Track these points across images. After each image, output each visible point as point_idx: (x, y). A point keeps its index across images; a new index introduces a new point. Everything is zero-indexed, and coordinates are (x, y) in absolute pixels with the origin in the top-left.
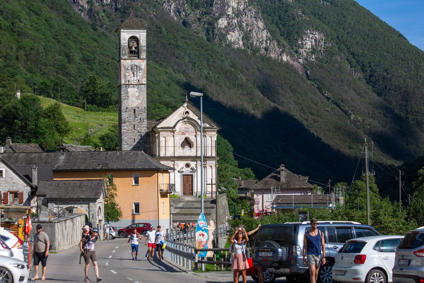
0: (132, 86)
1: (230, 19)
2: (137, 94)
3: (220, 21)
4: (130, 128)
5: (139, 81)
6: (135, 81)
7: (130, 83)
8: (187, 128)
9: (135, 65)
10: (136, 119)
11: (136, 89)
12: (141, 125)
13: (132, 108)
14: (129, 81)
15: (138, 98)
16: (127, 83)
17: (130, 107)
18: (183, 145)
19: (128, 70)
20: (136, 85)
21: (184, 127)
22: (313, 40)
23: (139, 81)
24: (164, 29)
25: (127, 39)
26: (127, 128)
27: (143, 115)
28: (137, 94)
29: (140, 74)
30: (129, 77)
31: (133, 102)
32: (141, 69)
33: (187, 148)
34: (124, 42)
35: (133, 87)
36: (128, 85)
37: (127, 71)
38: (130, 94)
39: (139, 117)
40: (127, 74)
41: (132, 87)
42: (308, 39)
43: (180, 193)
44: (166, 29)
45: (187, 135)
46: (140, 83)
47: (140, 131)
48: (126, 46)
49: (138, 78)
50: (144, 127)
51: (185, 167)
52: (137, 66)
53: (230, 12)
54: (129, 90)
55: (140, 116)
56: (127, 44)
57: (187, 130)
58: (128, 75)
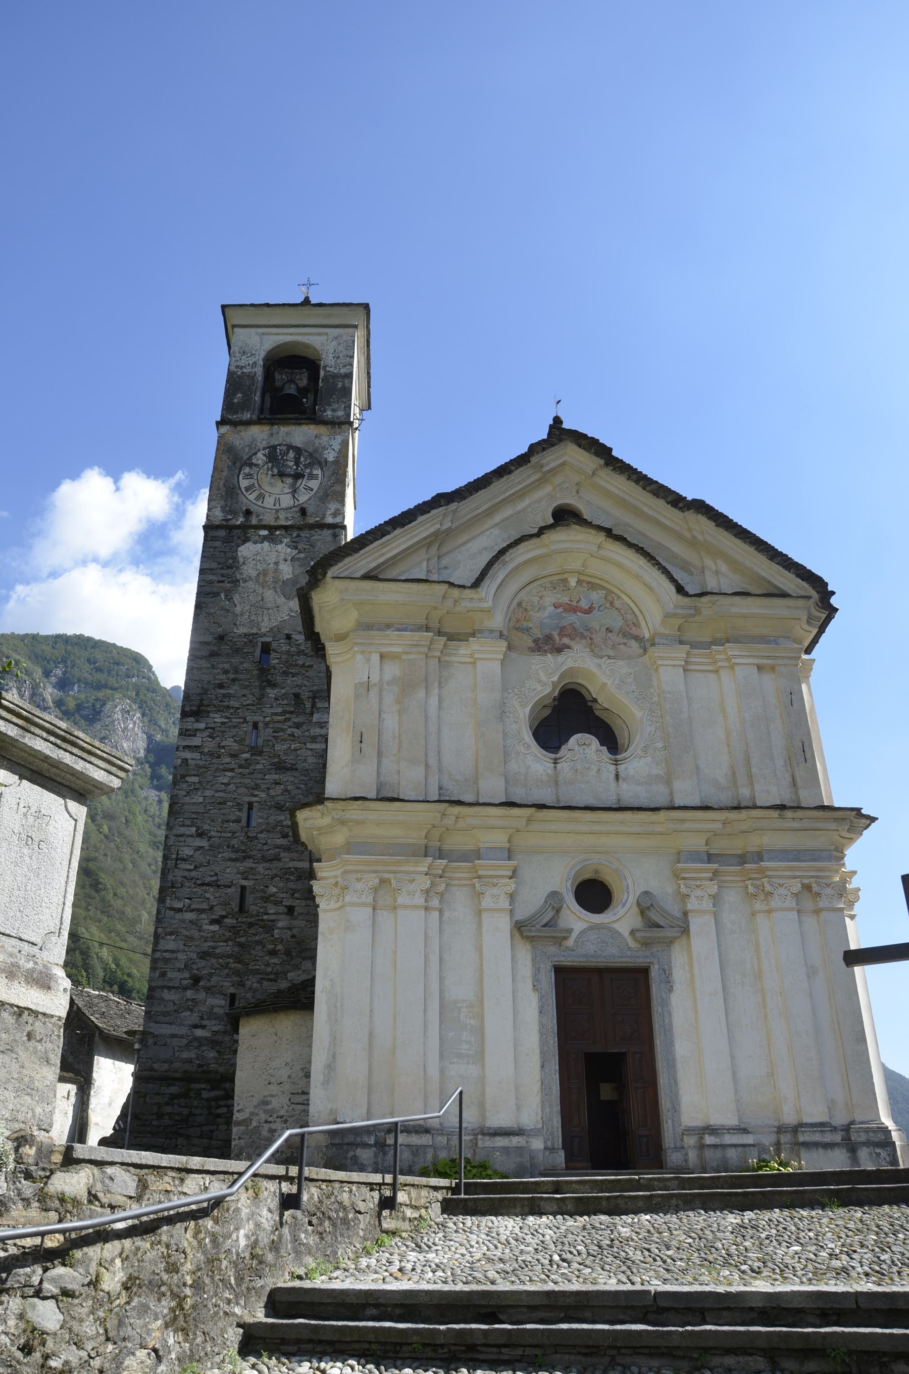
0: (265, 533)
4: (229, 742)
5: (303, 512)
6: (282, 515)
7: (254, 521)
8: (574, 610)
9: (290, 447)
10: (272, 693)
11: (283, 549)
12: (298, 726)
13: (251, 638)
14: (248, 513)
16: (240, 520)
17: (242, 630)
19: (251, 465)
20: (286, 528)
21: (550, 599)
23: (303, 512)
25: (263, 354)
26: (210, 745)
27: (310, 673)
29: (314, 484)
30: (252, 497)
31: (261, 606)
33: (583, 748)
34: (241, 364)
35: (271, 539)
36: (245, 527)
37: (247, 470)
38: (249, 570)
40: (244, 483)
41: (265, 538)
43: (537, 1144)
46: (311, 521)
47: (290, 759)
48: (252, 377)
49: (303, 498)
50: (314, 739)
51: (570, 900)
52: (298, 451)
54: (246, 550)
55: (298, 680)
56: (259, 371)
57: (572, 618)
58: (248, 489)
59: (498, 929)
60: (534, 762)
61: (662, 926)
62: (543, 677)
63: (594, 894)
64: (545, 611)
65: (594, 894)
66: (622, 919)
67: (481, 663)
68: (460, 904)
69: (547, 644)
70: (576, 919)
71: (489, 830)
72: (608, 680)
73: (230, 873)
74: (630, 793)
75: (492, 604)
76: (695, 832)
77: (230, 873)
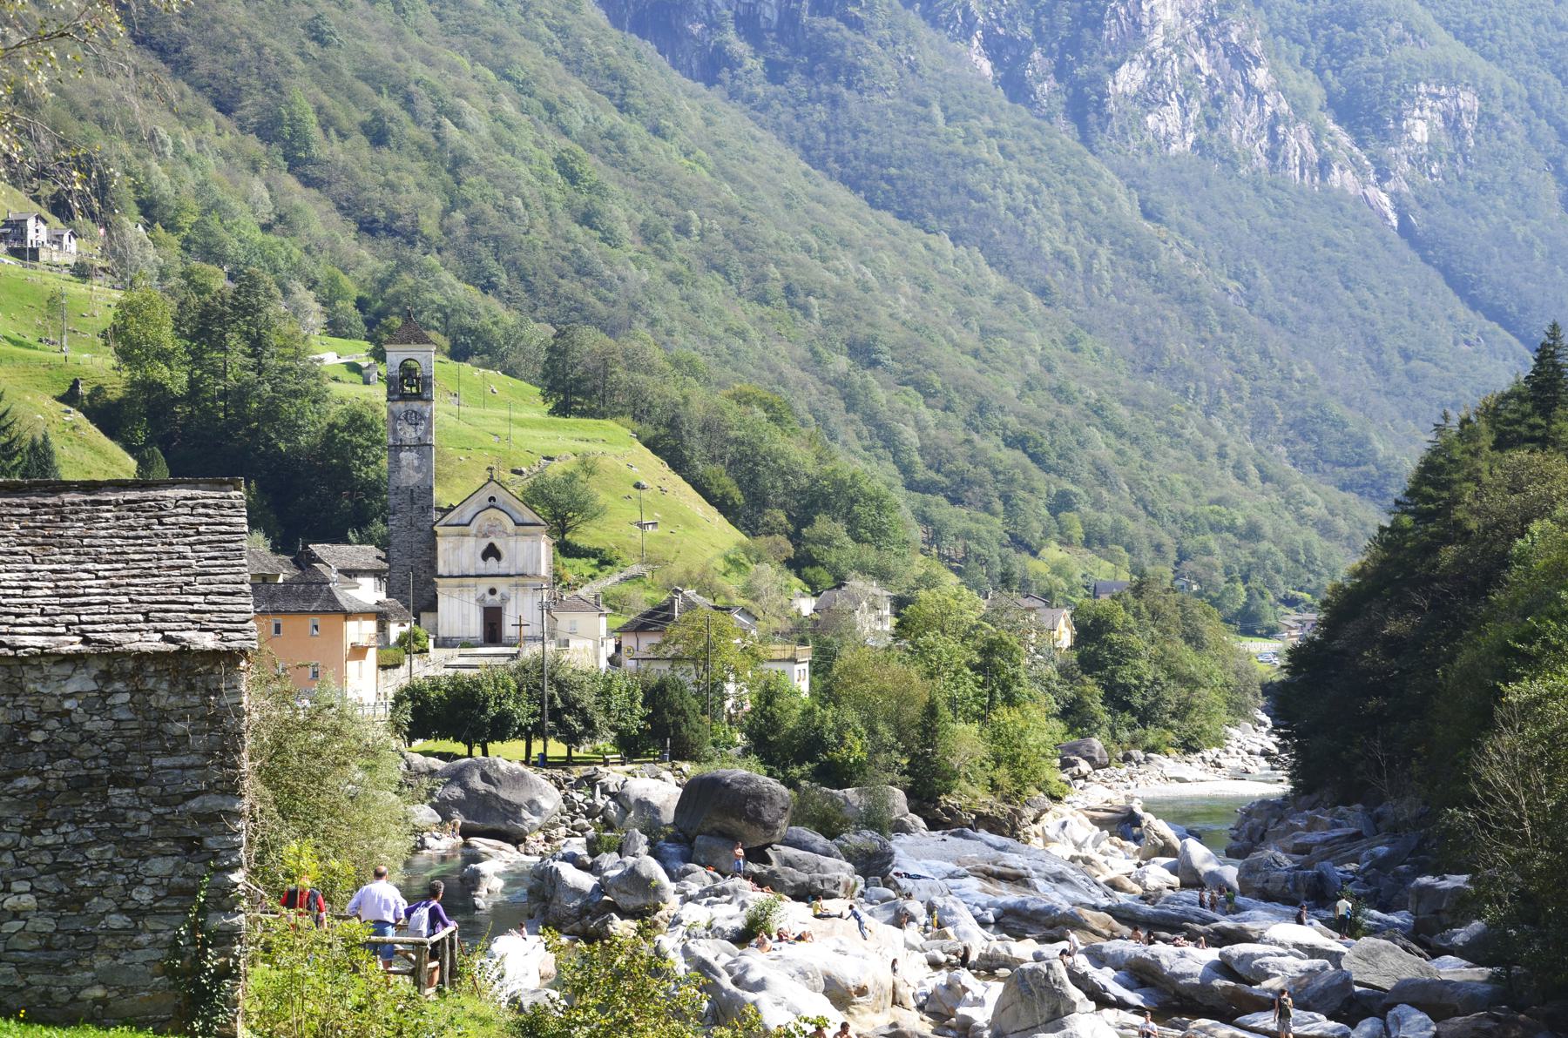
1: (1154, 62)
2: (416, 463)
3: (1123, 73)
11: (414, 454)
15: (418, 469)
18: (485, 556)
22: (1438, 117)
24: (936, 110)
28: (416, 463)
31: (409, 476)
32: (423, 418)
33: (492, 560)
38: (404, 463)
39: (420, 503)
42: (1417, 113)
44: (945, 109)
45: (492, 539)
53: (1157, 40)
54: (402, 455)
59: (473, 600)
60: (481, 563)
61: (505, 599)
62: (484, 544)
63: (493, 592)
64: (485, 528)
65: (493, 592)
66: (497, 597)
67: (470, 542)
68: (465, 597)
69: (486, 536)
70: (489, 598)
71: (472, 581)
72: (499, 544)
73: (408, 562)
74: (502, 571)
75: (473, 529)
76: (512, 580)
77: (408, 562)
